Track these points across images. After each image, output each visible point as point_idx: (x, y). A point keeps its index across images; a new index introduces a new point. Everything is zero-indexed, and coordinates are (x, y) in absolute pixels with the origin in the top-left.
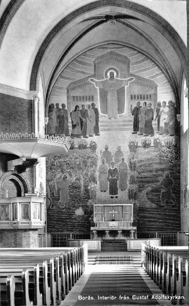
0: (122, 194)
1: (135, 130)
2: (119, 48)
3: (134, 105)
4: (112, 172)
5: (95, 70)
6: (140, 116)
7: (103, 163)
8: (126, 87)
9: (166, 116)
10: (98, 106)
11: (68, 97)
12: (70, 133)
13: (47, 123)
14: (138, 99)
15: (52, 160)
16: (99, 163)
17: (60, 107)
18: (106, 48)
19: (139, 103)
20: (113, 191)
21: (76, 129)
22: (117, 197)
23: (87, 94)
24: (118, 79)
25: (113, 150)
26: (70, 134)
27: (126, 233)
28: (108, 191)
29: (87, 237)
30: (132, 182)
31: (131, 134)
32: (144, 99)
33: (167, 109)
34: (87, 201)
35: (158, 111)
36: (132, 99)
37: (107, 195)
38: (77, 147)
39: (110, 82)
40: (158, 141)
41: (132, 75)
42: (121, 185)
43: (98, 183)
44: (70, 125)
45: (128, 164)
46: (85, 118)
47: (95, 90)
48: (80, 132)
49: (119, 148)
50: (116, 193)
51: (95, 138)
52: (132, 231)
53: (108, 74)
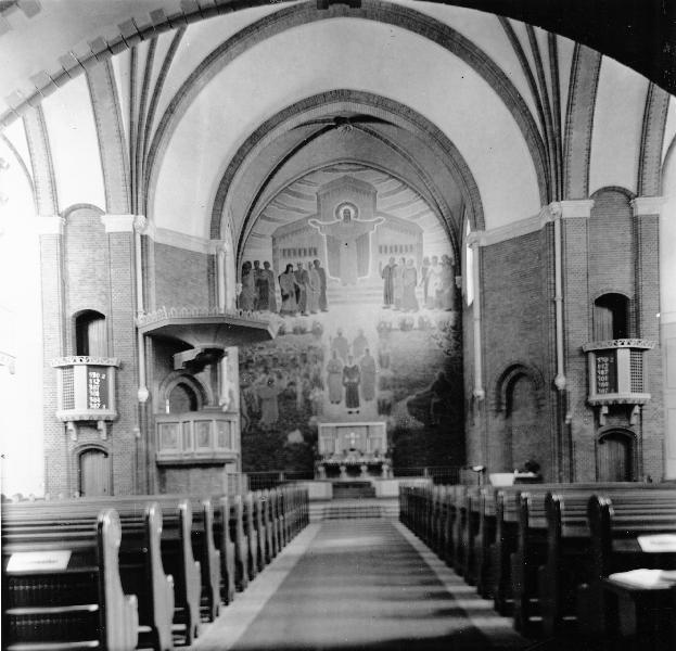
0: (367, 407)
1: (387, 302)
2: (359, 170)
3: (386, 263)
4: (349, 372)
5: (319, 205)
6: (394, 279)
7: (335, 357)
8: (371, 233)
9: (439, 280)
10: (325, 264)
11: (274, 251)
13: (239, 294)
14: (391, 251)
15: (250, 353)
16: (328, 357)
17: (262, 267)
18: (337, 170)
19: (393, 260)
20: (352, 400)
21: (288, 302)
22: (358, 412)
23: (306, 245)
24: (358, 220)
25: (350, 336)
26: (278, 309)
27: (375, 469)
28: (343, 402)
29: (310, 475)
30: (384, 387)
32: (401, 251)
33: (439, 269)
34: (308, 420)
35: (425, 270)
36: (381, 252)
37: (342, 408)
38: (291, 330)
39: (344, 225)
40: (425, 320)
41: (380, 214)
42: (364, 390)
43: (327, 389)
44: (278, 295)
45: (374, 355)
47: (320, 238)
48: (296, 306)
49: (361, 332)
50: (356, 404)
51: (320, 316)
52: (385, 467)
53: (341, 212)
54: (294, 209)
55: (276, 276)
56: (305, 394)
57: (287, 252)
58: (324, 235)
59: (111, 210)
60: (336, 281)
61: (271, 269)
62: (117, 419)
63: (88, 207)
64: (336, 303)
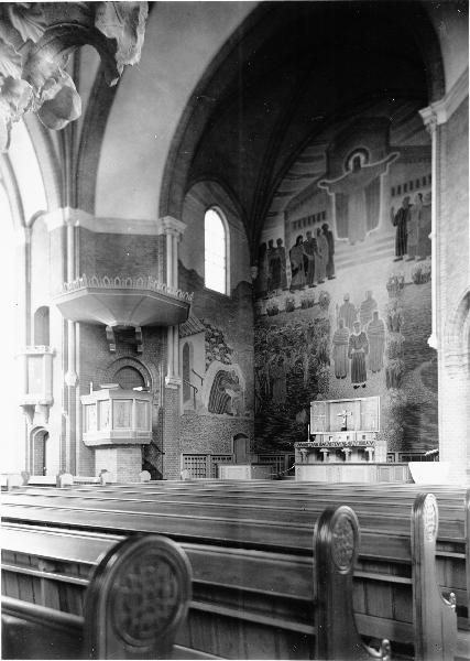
0: (376, 380)
6: (408, 223)
7: (341, 327)
8: (382, 176)
10: (333, 229)
11: (286, 226)
12: (289, 284)
13: (254, 276)
14: (405, 191)
16: (334, 329)
17: (275, 245)
22: (364, 386)
24: (369, 165)
26: (289, 284)
28: (349, 378)
30: (394, 354)
31: (391, 262)
36: (393, 194)
43: (332, 363)
44: (289, 271)
46: (312, 253)
47: (329, 198)
48: (304, 279)
49: (369, 294)
53: (351, 163)
54: (304, 176)
55: (287, 251)
56: (313, 370)
57: (298, 225)
58: (333, 195)
60: (344, 242)
61: (283, 245)
64: (344, 266)
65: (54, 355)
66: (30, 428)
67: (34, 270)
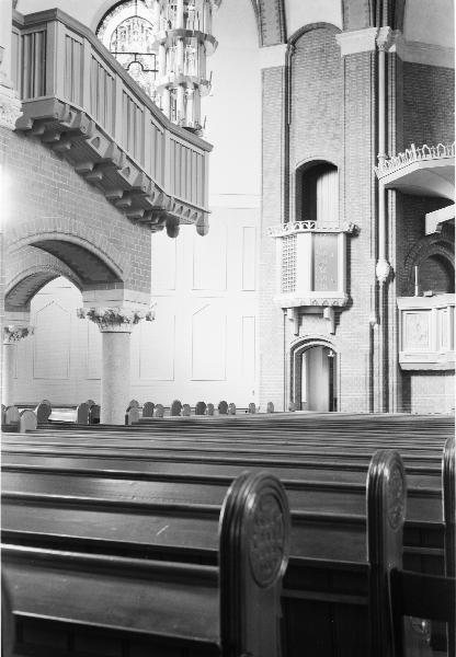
59: (349, 25)
62: (349, 304)
63: (322, 26)
65: (352, 235)
66: (292, 340)
67: (296, 106)
